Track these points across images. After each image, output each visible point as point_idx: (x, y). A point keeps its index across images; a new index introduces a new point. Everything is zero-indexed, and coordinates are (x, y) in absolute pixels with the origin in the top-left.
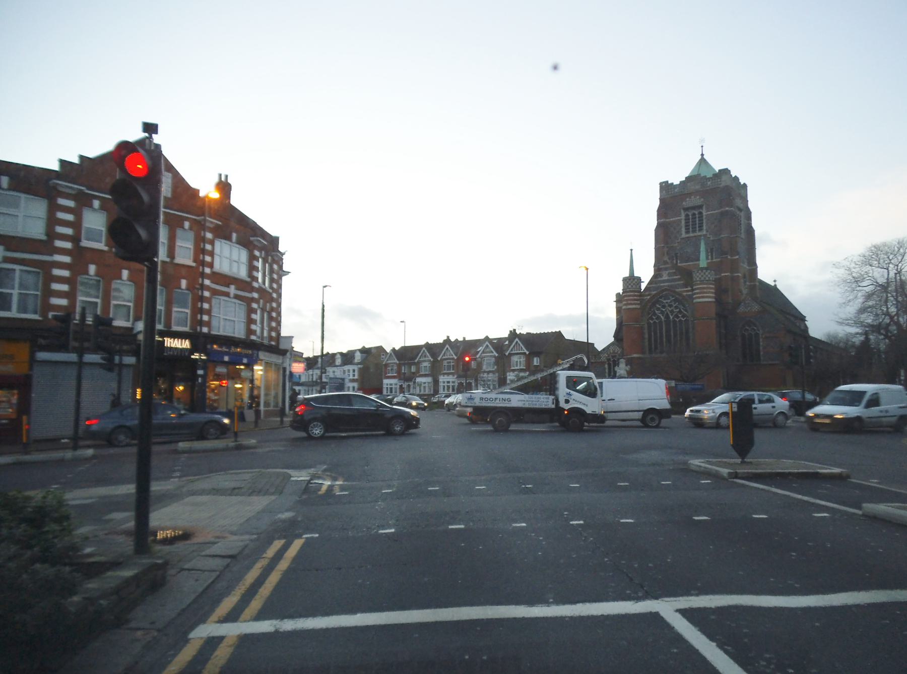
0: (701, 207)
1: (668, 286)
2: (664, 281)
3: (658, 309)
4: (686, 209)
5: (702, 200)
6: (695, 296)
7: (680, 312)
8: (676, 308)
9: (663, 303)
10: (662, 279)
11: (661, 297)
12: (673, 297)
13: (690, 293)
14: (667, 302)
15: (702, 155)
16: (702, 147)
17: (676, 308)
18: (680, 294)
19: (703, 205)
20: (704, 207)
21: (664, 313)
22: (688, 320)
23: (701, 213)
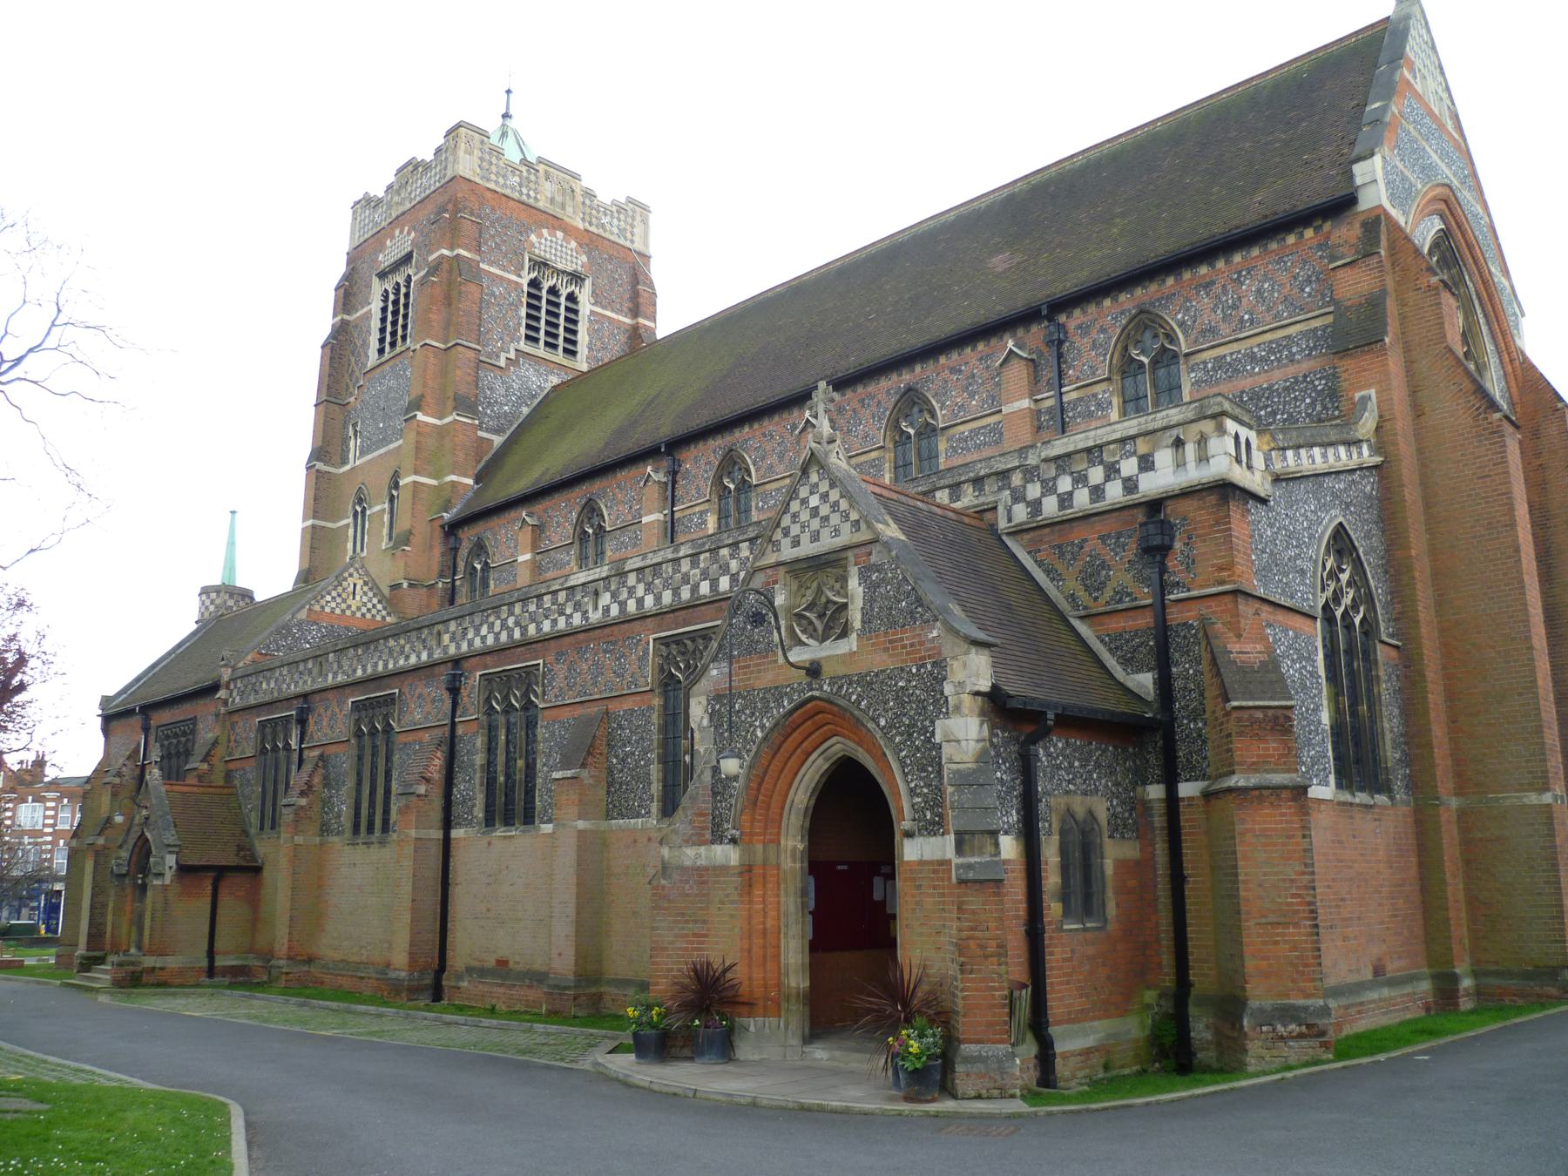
15: (506, 116)
16: (508, 92)
20: (588, 283)
23: (571, 298)
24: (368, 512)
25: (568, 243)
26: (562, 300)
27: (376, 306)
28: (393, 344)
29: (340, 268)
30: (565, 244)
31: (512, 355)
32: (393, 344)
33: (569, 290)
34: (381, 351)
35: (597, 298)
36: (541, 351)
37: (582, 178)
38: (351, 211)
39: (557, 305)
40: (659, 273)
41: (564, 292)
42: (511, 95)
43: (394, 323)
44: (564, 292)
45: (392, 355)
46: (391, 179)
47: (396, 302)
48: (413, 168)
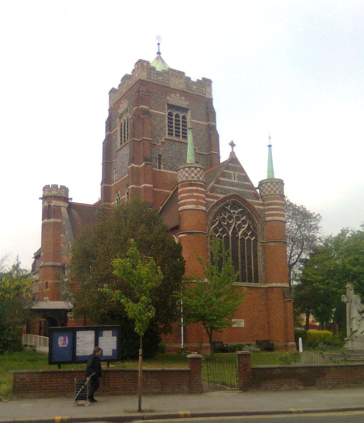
0: (185, 110)
1: (238, 192)
2: (233, 185)
3: (224, 219)
4: (170, 106)
5: (187, 103)
6: (267, 213)
7: (248, 229)
8: (244, 222)
9: (230, 213)
10: (231, 180)
11: (227, 205)
12: (240, 208)
13: (262, 207)
14: (234, 213)
15: (159, 53)
16: (159, 44)
17: (244, 222)
18: (249, 205)
19: (189, 109)
20: (189, 112)
21: (230, 226)
22: (257, 241)
23: (184, 117)
24: (121, 199)
25: (181, 98)
26: (181, 119)
27: (118, 128)
28: (125, 141)
29: (106, 115)
30: (180, 98)
31: (163, 141)
32: (125, 141)
33: (183, 115)
34: (121, 143)
35: (193, 117)
36: (174, 138)
37: (185, 73)
38: (108, 95)
39: (179, 121)
40: (216, 105)
41: (181, 116)
42: (160, 46)
43: (125, 133)
44: (181, 116)
45: (125, 144)
46: (120, 82)
47: (124, 126)
48: (126, 78)
